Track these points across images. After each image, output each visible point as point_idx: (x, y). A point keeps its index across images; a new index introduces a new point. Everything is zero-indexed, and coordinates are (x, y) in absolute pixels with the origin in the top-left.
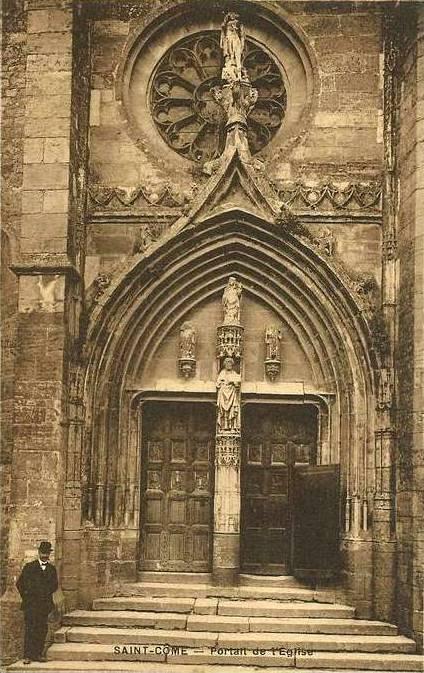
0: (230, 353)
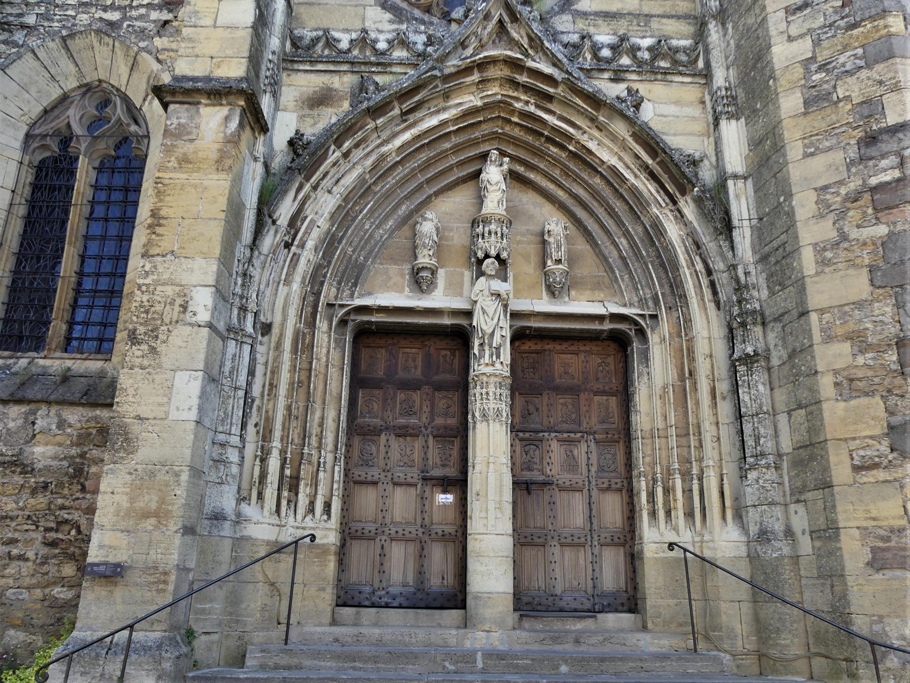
0: (493, 253)
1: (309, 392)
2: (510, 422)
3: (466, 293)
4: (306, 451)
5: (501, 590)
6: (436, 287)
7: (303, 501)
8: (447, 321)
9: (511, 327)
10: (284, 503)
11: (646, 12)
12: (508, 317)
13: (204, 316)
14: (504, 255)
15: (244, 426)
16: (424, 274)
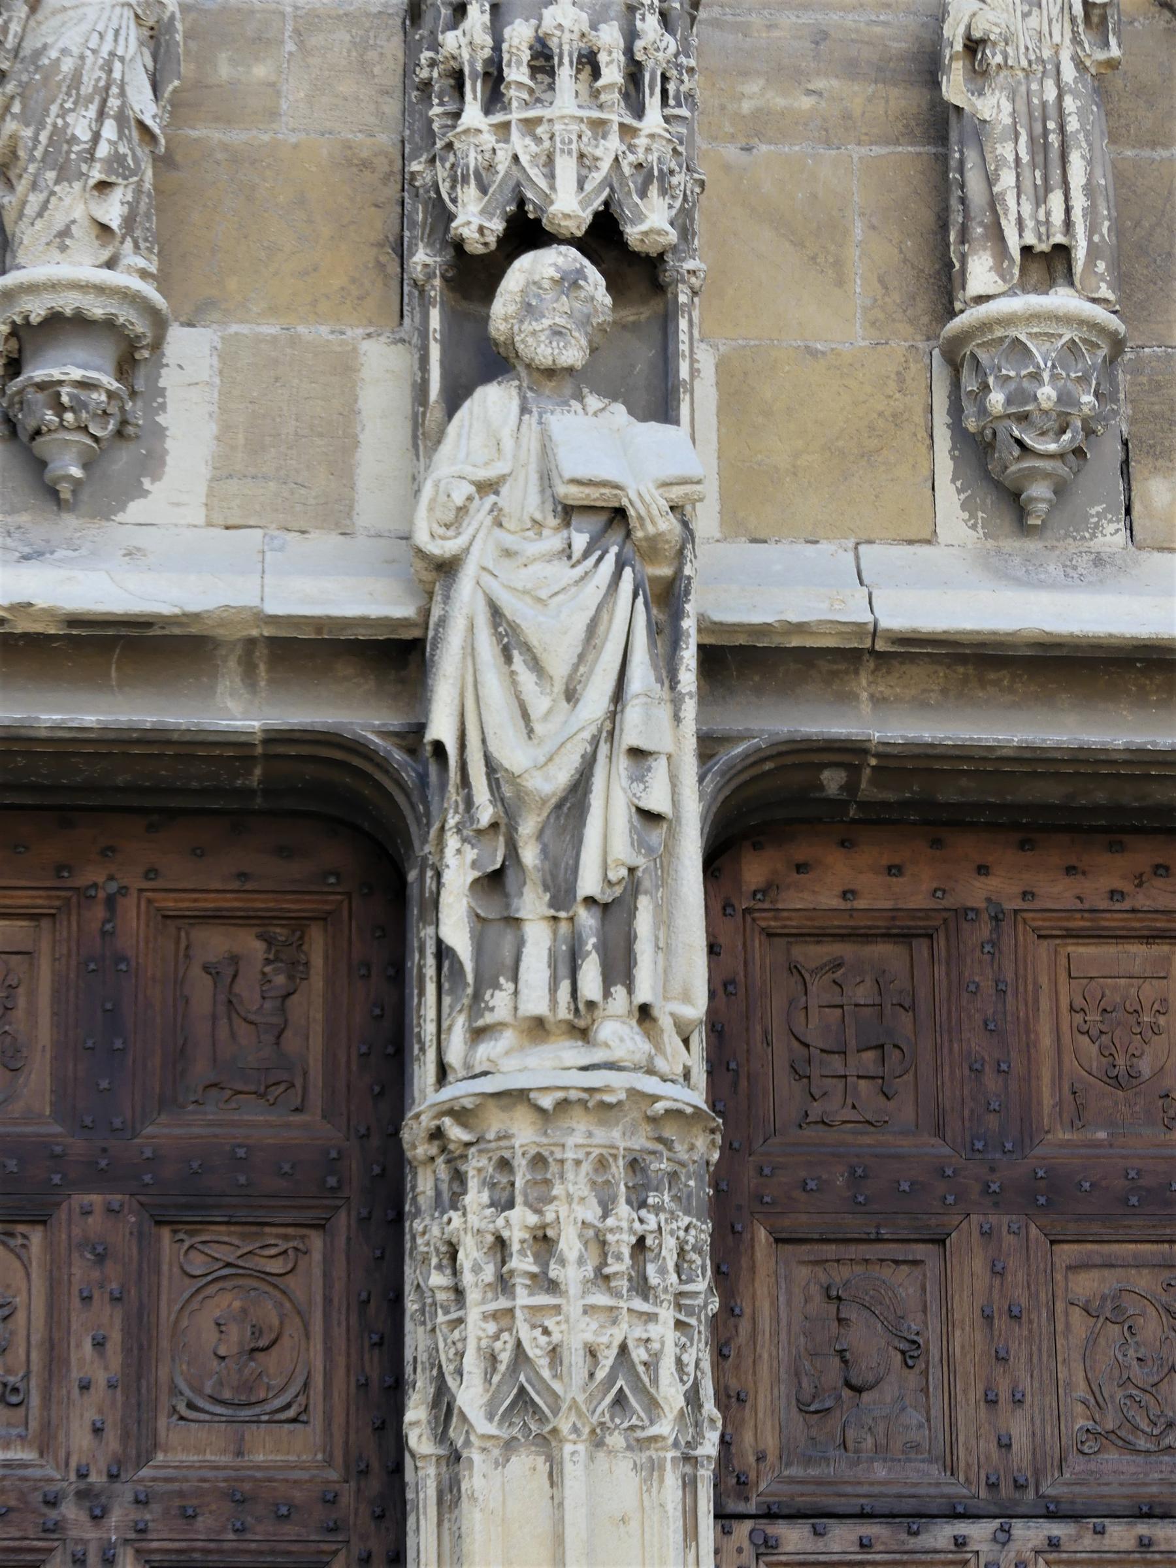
0: (569, 207)
2: (709, 1447)
3: (372, 505)
6: (153, 464)
8: (237, 711)
12: (688, 678)
14: (650, 222)
16: (64, 366)
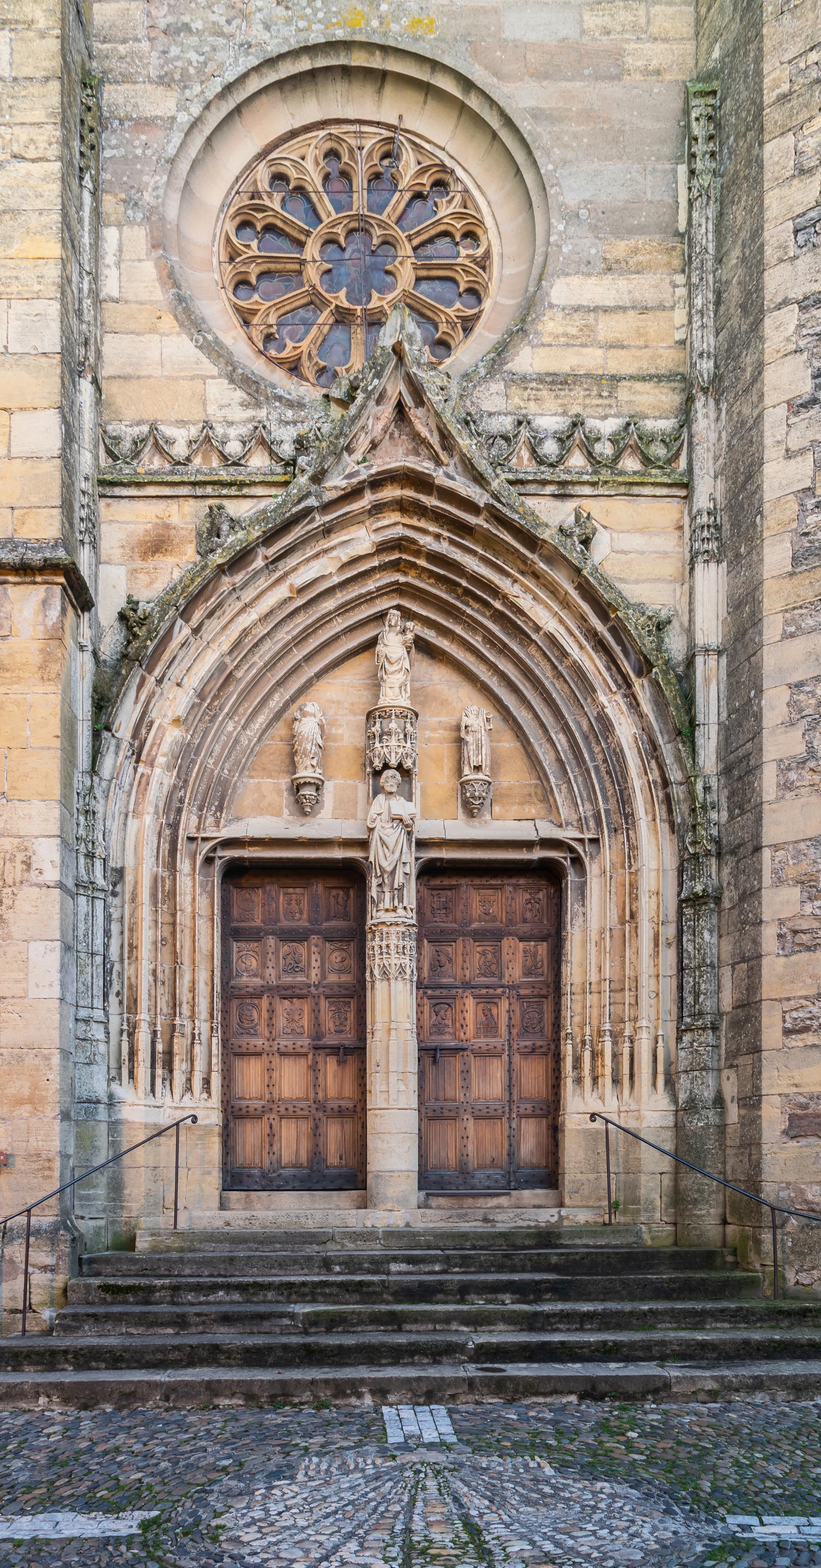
0: (394, 762)
1: (175, 952)
3: (360, 815)
4: (178, 1021)
5: (404, 1168)
7: (179, 1078)
8: (338, 854)
9: (417, 859)
10: (158, 1081)
11: (614, 372)
13: (52, 875)
14: (408, 763)
15: (106, 996)
16: (308, 791)
